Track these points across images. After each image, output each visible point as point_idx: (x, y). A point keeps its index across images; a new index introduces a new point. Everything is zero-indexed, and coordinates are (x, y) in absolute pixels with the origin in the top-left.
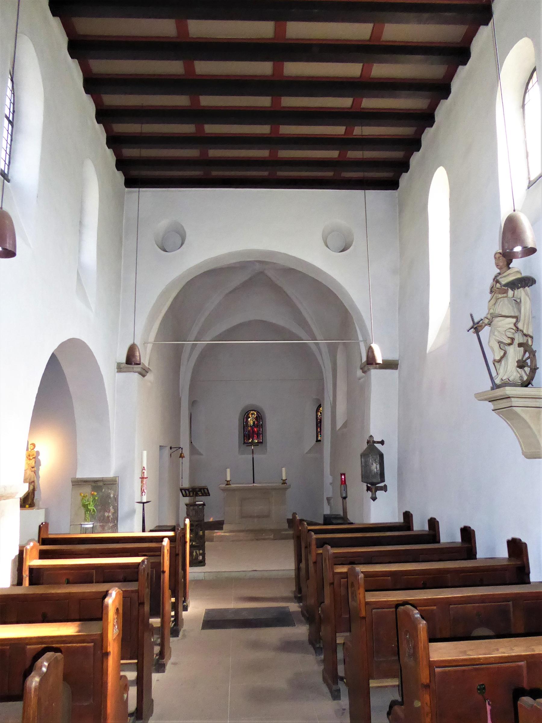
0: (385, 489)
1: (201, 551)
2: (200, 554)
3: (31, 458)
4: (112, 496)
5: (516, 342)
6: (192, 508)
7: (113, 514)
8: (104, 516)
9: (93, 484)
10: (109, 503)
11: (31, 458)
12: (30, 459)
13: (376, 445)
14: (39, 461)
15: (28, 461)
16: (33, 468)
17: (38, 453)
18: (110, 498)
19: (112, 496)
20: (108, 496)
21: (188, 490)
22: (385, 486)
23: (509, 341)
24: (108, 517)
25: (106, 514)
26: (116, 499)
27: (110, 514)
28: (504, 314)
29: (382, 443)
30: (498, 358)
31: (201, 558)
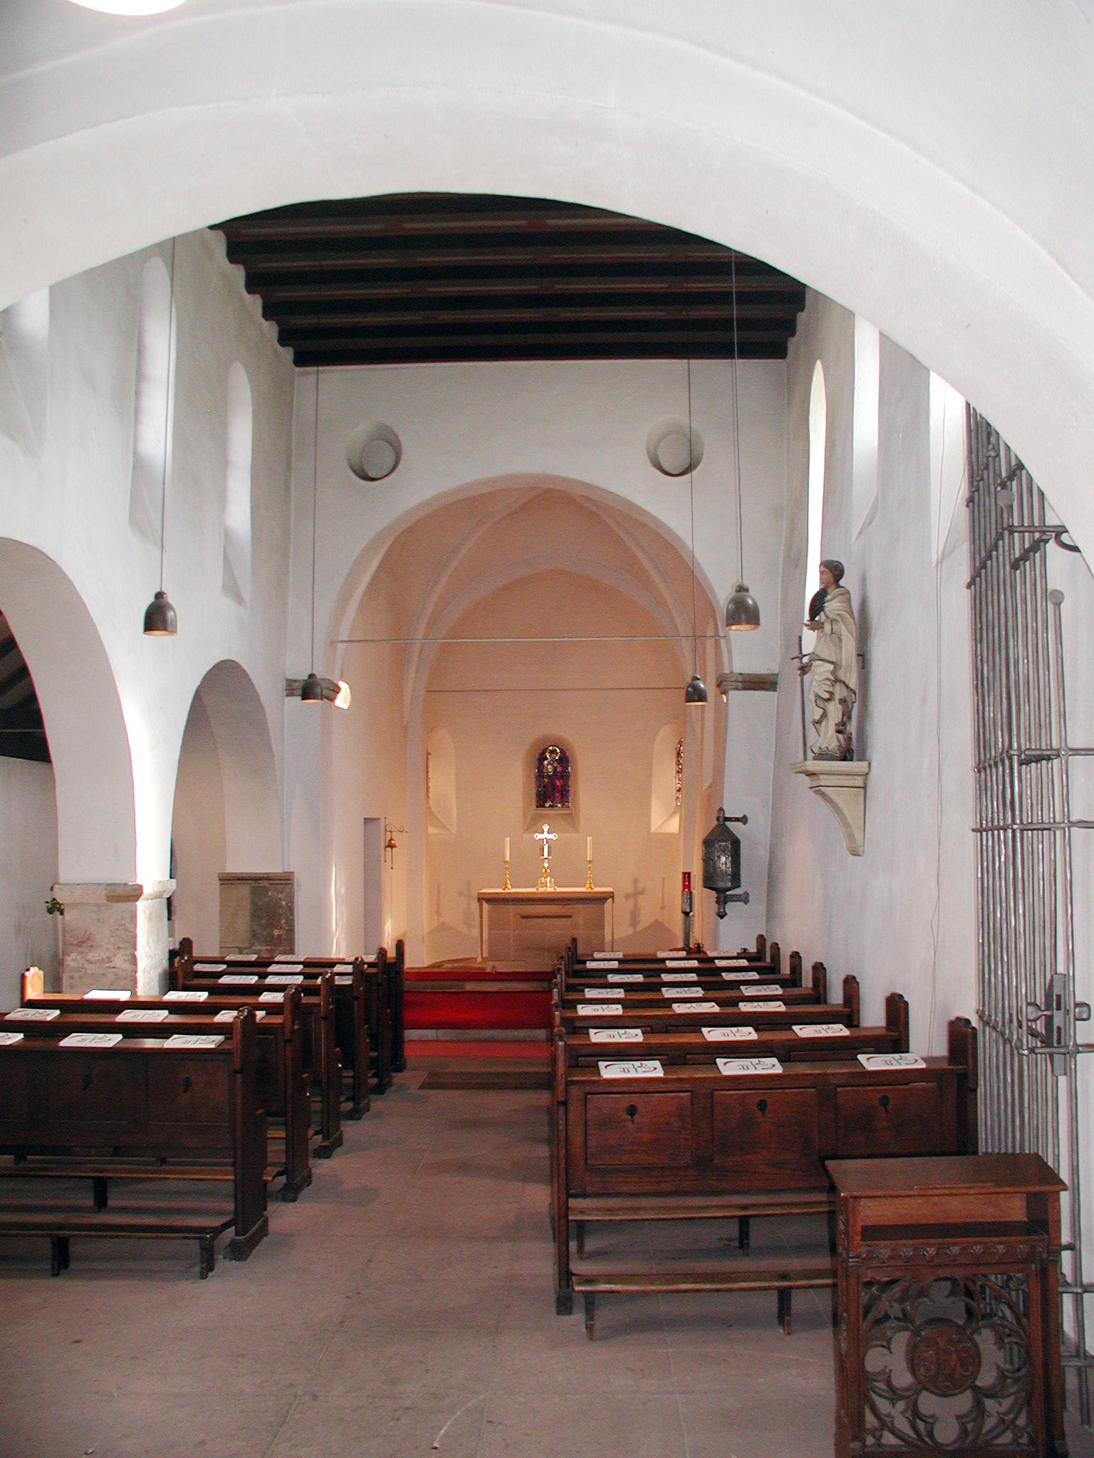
0: (745, 899)
5: (837, 697)
8: (273, 936)
9: (253, 884)
13: (728, 824)
18: (281, 906)
22: (747, 894)
23: (826, 696)
24: (280, 936)
26: (291, 909)
28: (823, 657)
29: (744, 820)
30: (817, 718)
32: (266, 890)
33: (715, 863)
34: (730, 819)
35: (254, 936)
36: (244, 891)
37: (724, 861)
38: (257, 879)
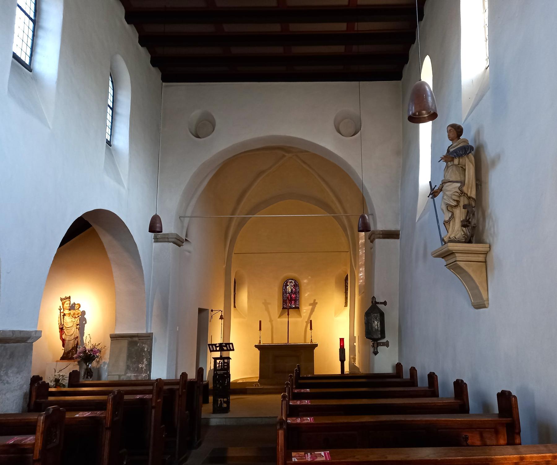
1: (225, 400)
2: (224, 402)
3: (77, 316)
4: (146, 349)
6: (218, 361)
7: (146, 366)
10: (143, 356)
11: (77, 316)
12: (75, 318)
14: (85, 320)
15: (73, 319)
16: (77, 325)
17: (84, 313)
18: (144, 351)
19: (146, 349)
20: (142, 350)
21: (215, 345)
24: (142, 368)
25: (140, 366)
27: (144, 366)
31: (225, 405)
32: (136, 343)
33: (372, 326)
34: (378, 303)
35: (128, 367)
36: (124, 343)
37: (376, 324)
38: (131, 336)
